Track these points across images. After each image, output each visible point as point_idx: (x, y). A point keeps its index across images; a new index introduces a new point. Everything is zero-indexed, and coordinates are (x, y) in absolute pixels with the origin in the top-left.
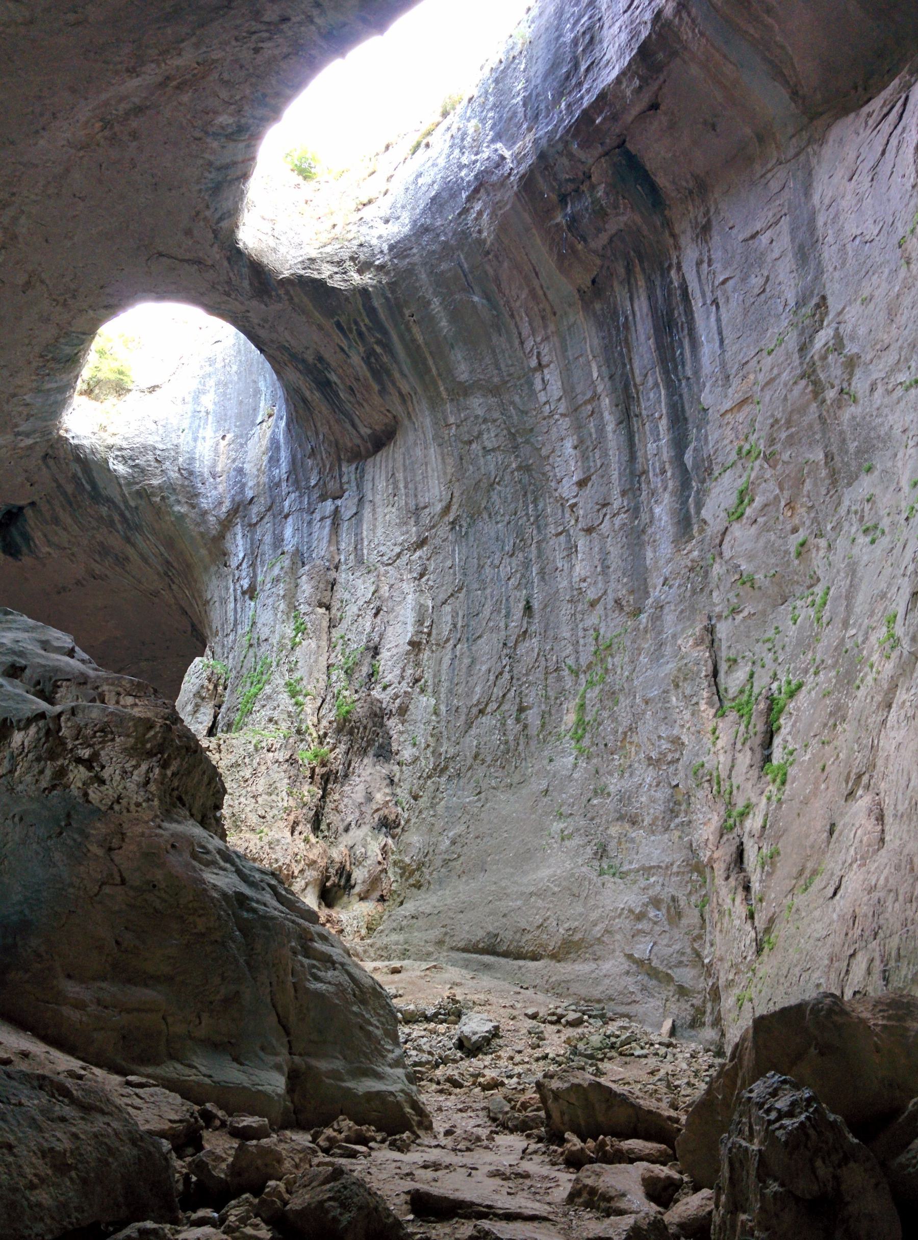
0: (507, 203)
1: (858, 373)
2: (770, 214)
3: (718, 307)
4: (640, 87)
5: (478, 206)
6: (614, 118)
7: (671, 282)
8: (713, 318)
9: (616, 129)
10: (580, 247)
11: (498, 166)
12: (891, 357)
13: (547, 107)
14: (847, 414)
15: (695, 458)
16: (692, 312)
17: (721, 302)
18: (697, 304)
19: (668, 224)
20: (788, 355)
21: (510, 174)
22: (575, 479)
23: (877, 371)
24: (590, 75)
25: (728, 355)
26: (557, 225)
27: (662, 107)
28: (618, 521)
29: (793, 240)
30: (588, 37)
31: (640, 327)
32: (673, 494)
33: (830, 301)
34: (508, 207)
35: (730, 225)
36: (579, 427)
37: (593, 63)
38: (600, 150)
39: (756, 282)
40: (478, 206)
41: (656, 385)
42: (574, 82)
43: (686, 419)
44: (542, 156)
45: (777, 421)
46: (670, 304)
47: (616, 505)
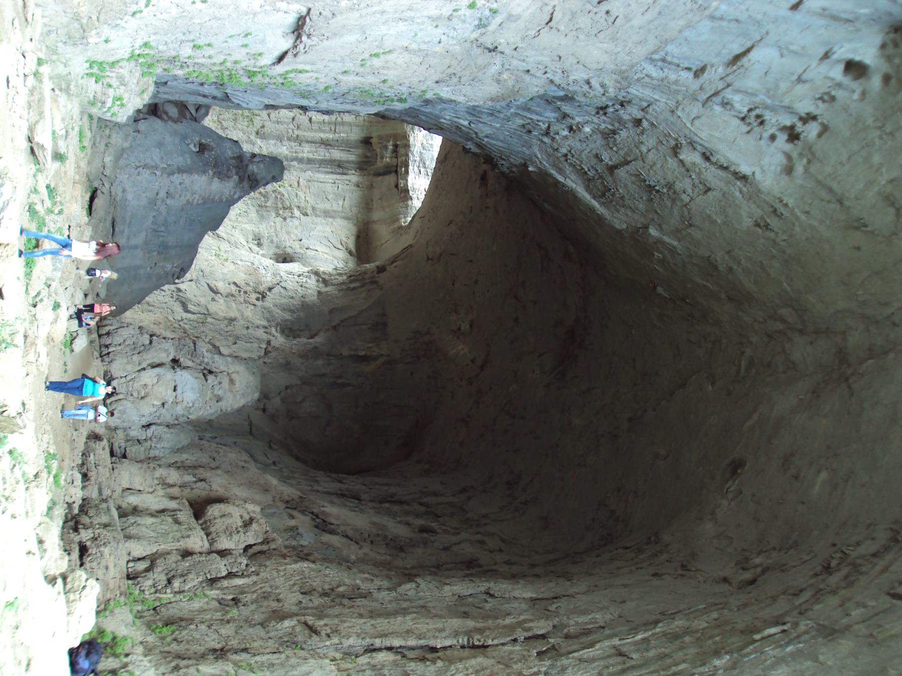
1: (281, 219)
8: (331, 181)
10: (380, 145)
12: (278, 229)
14: (274, 215)
18: (339, 177)
19: (369, 175)
20: (300, 202)
22: (314, 117)
23: (278, 226)
24: (418, 171)
25: (316, 184)
28: (290, 131)
29: (333, 211)
32: (287, 155)
33: (306, 217)
36: (329, 123)
39: (330, 197)
41: (325, 156)
45: (283, 195)
47: (296, 132)
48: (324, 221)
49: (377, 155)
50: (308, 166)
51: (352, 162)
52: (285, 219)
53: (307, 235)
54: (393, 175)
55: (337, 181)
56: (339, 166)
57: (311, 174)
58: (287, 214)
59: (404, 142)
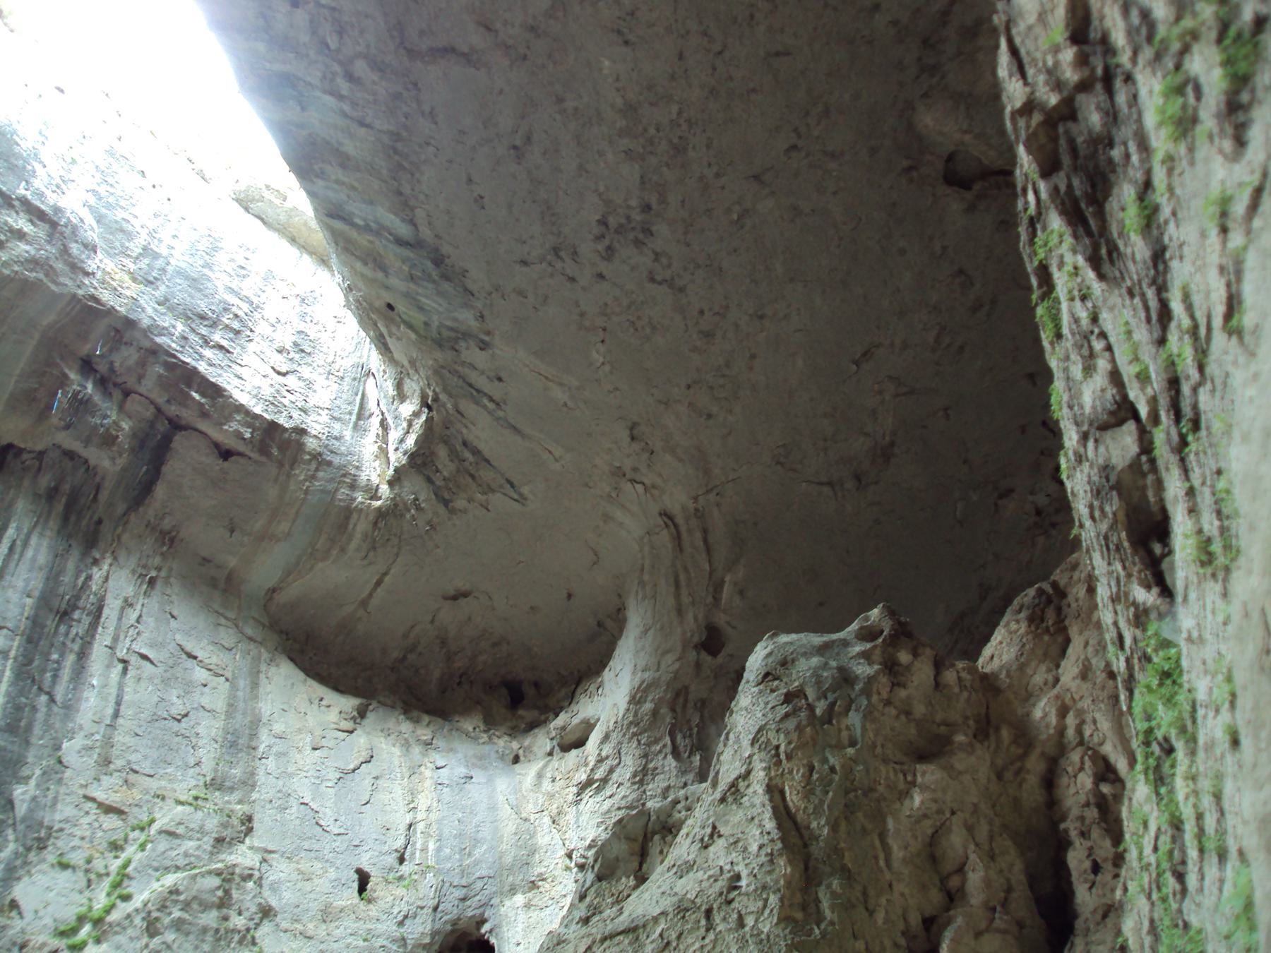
0: (57, 284)
1: (267, 927)
2: (214, 660)
3: (125, 671)
4: (245, 439)
5: (28, 228)
6: (204, 415)
7: (89, 578)
9: (187, 415)
11: (86, 246)
13: (167, 300)
15: (31, 810)
16: (93, 636)
17: (132, 672)
18: (103, 639)
20: (202, 831)
21: (87, 274)
25: (119, 738)
26: (66, 376)
27: (226, 464)
30: (236, 325)
31: (24, 567)
34: (53, 287)
35: (175, 613)
37: (229, 352)
38: (161, 400)
40: (21, 223)
42: (204, 331)
43: (27, 743)
44: (130, 324)
45: (174, 891)
46: (78, 597)
48: (271, 763)
49: (70, 455)
50: (38, 738)
51: (59, 557)
52: (267, 912)
53: (340, 843)
54: (179, 441)
55: (121, 653)
56: (64, 615)
57: (79, 742)
58: (246, 896)
59: (101, 326)
